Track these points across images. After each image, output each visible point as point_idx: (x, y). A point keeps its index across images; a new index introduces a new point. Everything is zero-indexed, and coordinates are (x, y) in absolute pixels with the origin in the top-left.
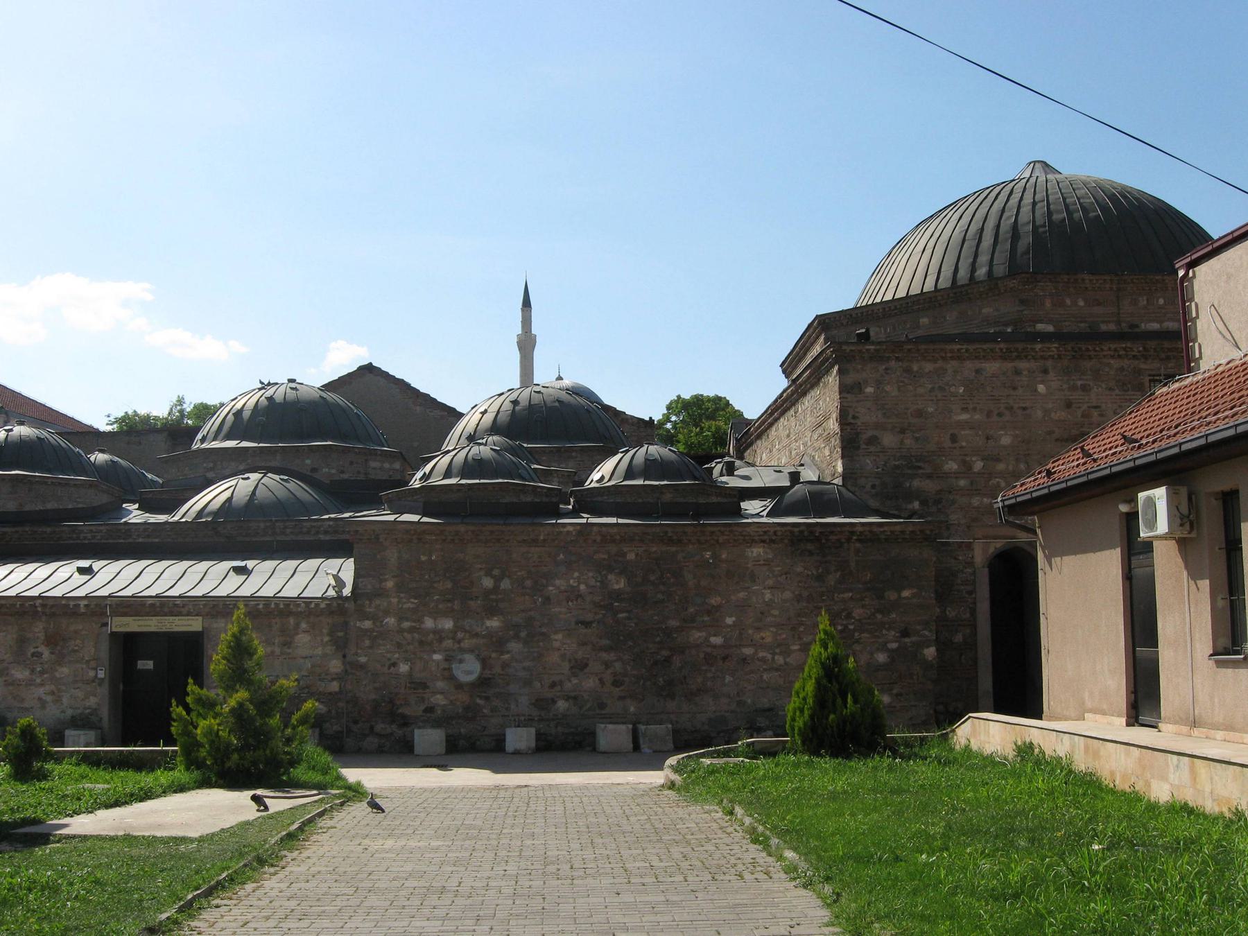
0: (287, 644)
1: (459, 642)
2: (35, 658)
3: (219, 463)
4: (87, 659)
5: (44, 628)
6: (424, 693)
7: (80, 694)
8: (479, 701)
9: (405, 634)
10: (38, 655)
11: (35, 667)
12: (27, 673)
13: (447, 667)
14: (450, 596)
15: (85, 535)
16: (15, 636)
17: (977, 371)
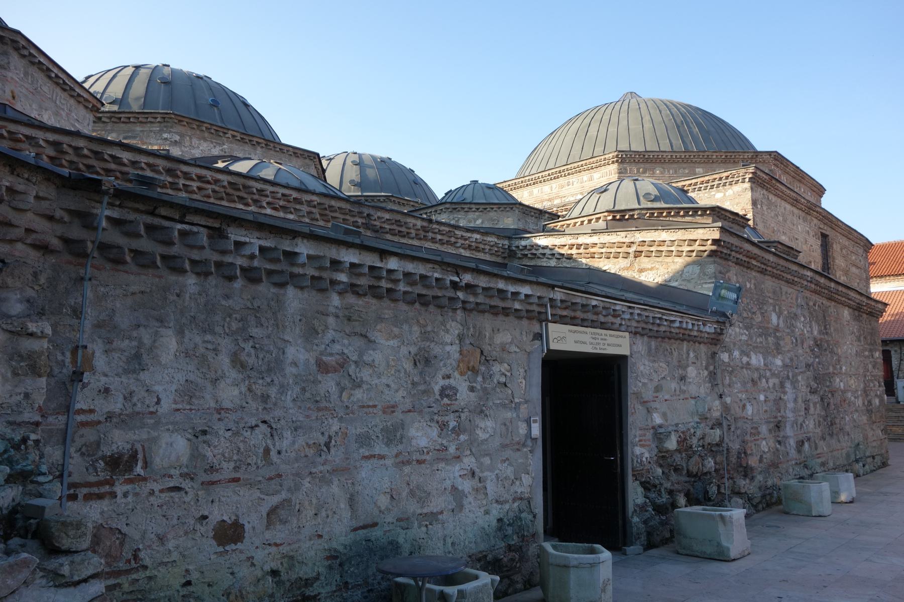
0: (683, 378)
1: (767, 382)
2: (446, 400)
3: (188, 138)
4: (517, 400)
5: (459, 335)
6: (758, 440)
7: (509, 472)
8: (778, 446)
9: (745, 370)
10: (448, 392)
11: (446, 418)
12: (434, 432)
13: (765, 408)
14: (761, 330)
15: (187, 183)
16: (414, 350)
17: (785, 209)
